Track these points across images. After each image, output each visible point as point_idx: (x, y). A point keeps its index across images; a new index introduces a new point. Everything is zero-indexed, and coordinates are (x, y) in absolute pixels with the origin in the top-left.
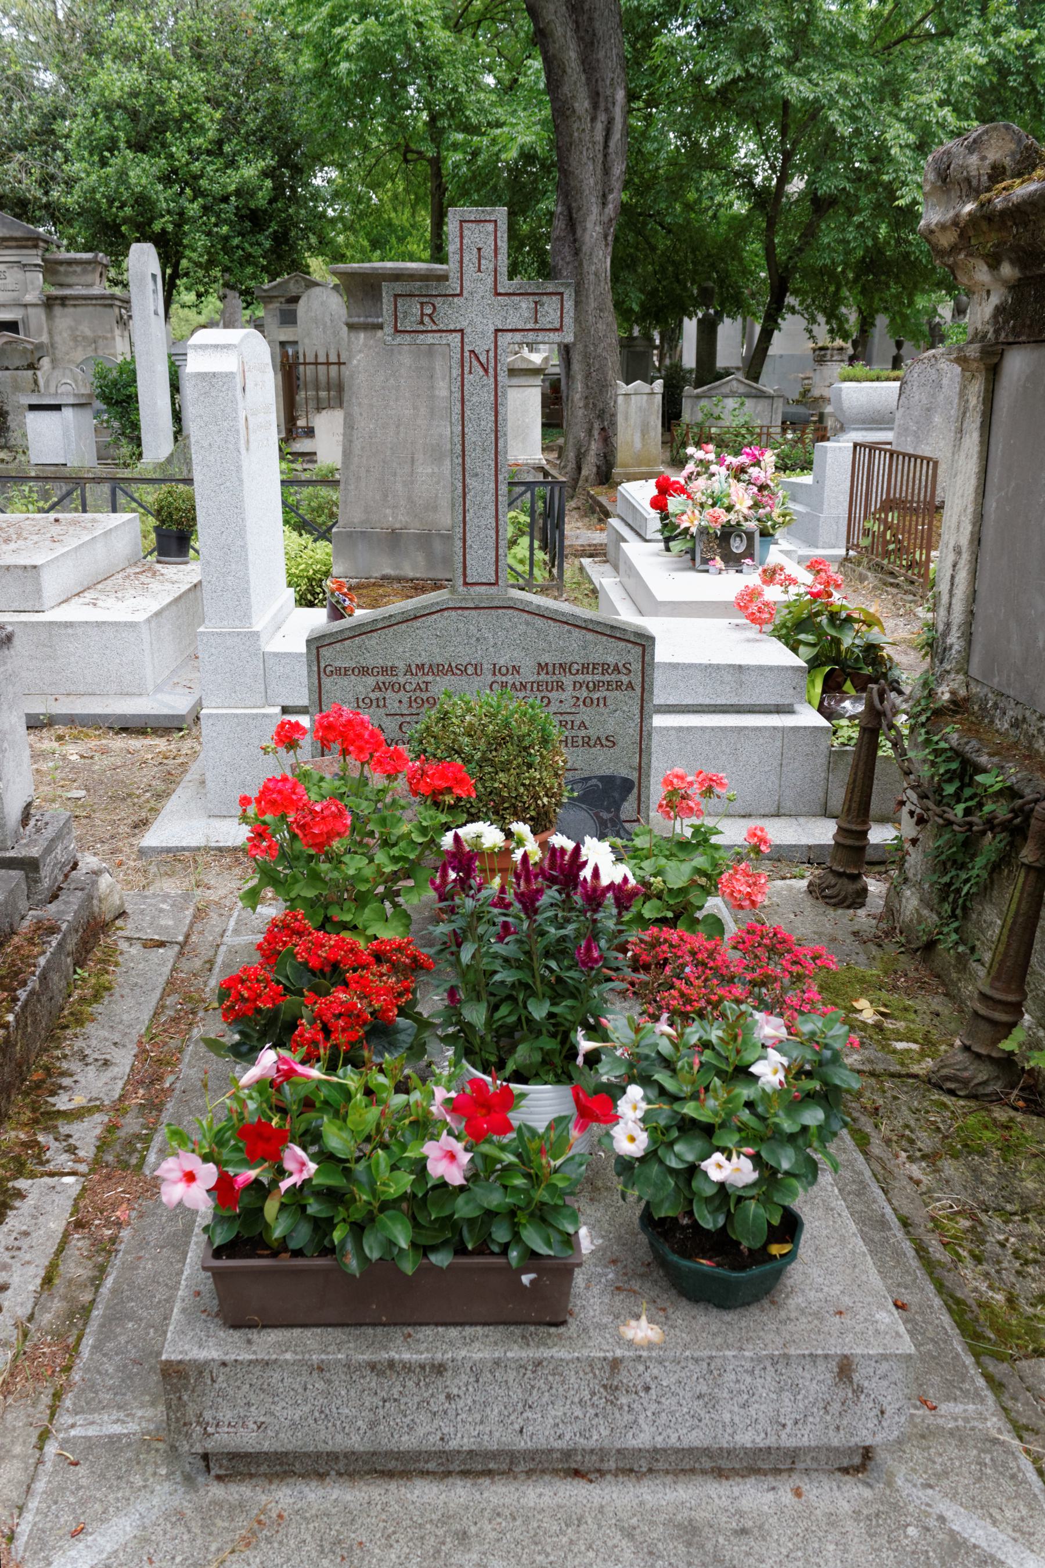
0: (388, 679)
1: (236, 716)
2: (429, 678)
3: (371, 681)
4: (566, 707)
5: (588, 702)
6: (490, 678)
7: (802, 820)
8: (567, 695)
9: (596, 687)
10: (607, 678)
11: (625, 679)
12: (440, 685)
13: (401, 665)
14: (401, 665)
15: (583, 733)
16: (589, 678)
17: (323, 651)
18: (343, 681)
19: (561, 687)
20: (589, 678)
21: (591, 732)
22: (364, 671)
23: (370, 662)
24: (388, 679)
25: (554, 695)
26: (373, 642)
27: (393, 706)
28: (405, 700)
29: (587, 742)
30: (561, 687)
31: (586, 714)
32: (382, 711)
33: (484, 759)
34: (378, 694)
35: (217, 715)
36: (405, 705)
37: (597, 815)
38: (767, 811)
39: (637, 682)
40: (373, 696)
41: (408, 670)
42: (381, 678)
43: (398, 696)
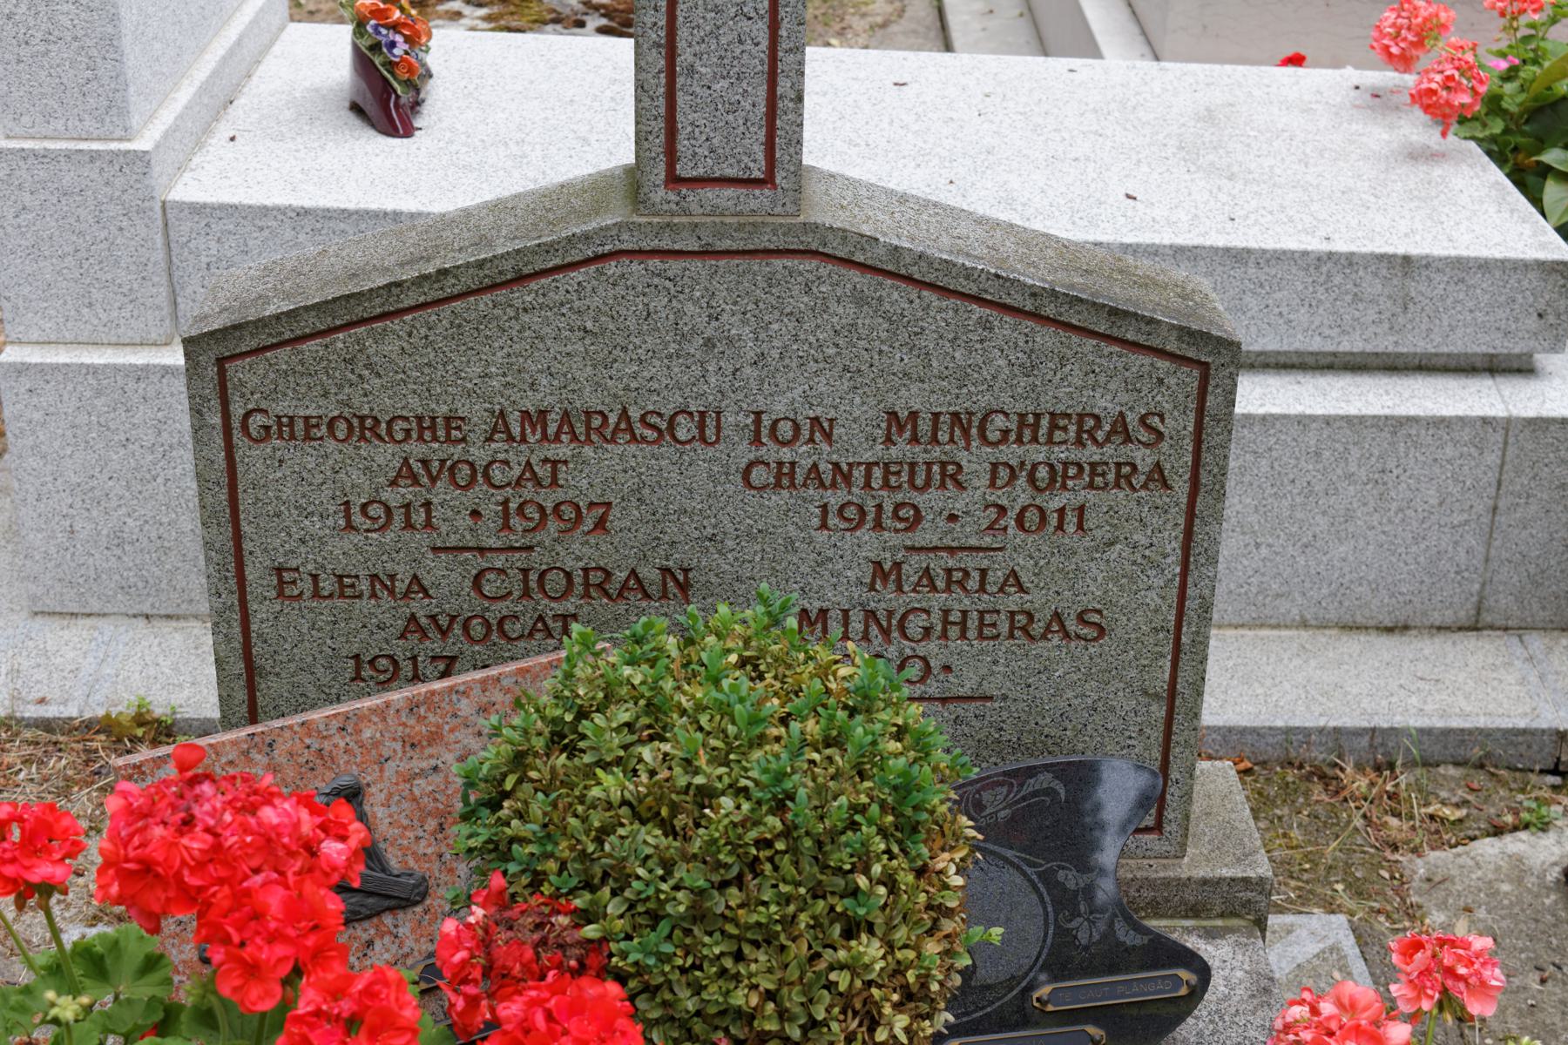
0: (437, 451)
1: (93, 370)
2: (563, 450)
3: (386, 455)
4: (967, 533)
5: (1031, 520)
6: (744, 453)
7: (1536, 642)
8: (973, 498)
9: (1058, 477)
10: (1091, 453)
11: (1143, 458)
12: (595, 470)
13: (477, 414)
14: (477, 414)
15: (1013, 601)
16: (1038, 453)
17: (237, 371)
18: (305, 457)
19: (953, 476)
20: (1038, 453)
21: (1036, 599)
22: (365, 428)
23: (385, 404)
24: (437, 451)
25: (930, 500)
26: (391, 347)
27: (454, 525)
28: (490, 509)
29: (1023, 626)
30: (953, 476)
31: (1022, 552)
32: (421, 539)
33: (698, 914)
34: (406, 492)
35: (41, 369)
36: (491, 522)
37: (1047, 877)
38: (1448, 617)
39: (1178, 464)
40: (392, 497)
41: (499, 425)
42: (416, 449)
43: (470, 498)
